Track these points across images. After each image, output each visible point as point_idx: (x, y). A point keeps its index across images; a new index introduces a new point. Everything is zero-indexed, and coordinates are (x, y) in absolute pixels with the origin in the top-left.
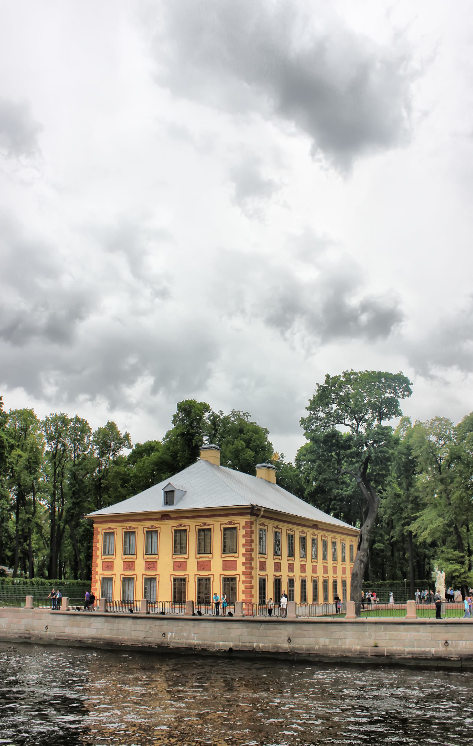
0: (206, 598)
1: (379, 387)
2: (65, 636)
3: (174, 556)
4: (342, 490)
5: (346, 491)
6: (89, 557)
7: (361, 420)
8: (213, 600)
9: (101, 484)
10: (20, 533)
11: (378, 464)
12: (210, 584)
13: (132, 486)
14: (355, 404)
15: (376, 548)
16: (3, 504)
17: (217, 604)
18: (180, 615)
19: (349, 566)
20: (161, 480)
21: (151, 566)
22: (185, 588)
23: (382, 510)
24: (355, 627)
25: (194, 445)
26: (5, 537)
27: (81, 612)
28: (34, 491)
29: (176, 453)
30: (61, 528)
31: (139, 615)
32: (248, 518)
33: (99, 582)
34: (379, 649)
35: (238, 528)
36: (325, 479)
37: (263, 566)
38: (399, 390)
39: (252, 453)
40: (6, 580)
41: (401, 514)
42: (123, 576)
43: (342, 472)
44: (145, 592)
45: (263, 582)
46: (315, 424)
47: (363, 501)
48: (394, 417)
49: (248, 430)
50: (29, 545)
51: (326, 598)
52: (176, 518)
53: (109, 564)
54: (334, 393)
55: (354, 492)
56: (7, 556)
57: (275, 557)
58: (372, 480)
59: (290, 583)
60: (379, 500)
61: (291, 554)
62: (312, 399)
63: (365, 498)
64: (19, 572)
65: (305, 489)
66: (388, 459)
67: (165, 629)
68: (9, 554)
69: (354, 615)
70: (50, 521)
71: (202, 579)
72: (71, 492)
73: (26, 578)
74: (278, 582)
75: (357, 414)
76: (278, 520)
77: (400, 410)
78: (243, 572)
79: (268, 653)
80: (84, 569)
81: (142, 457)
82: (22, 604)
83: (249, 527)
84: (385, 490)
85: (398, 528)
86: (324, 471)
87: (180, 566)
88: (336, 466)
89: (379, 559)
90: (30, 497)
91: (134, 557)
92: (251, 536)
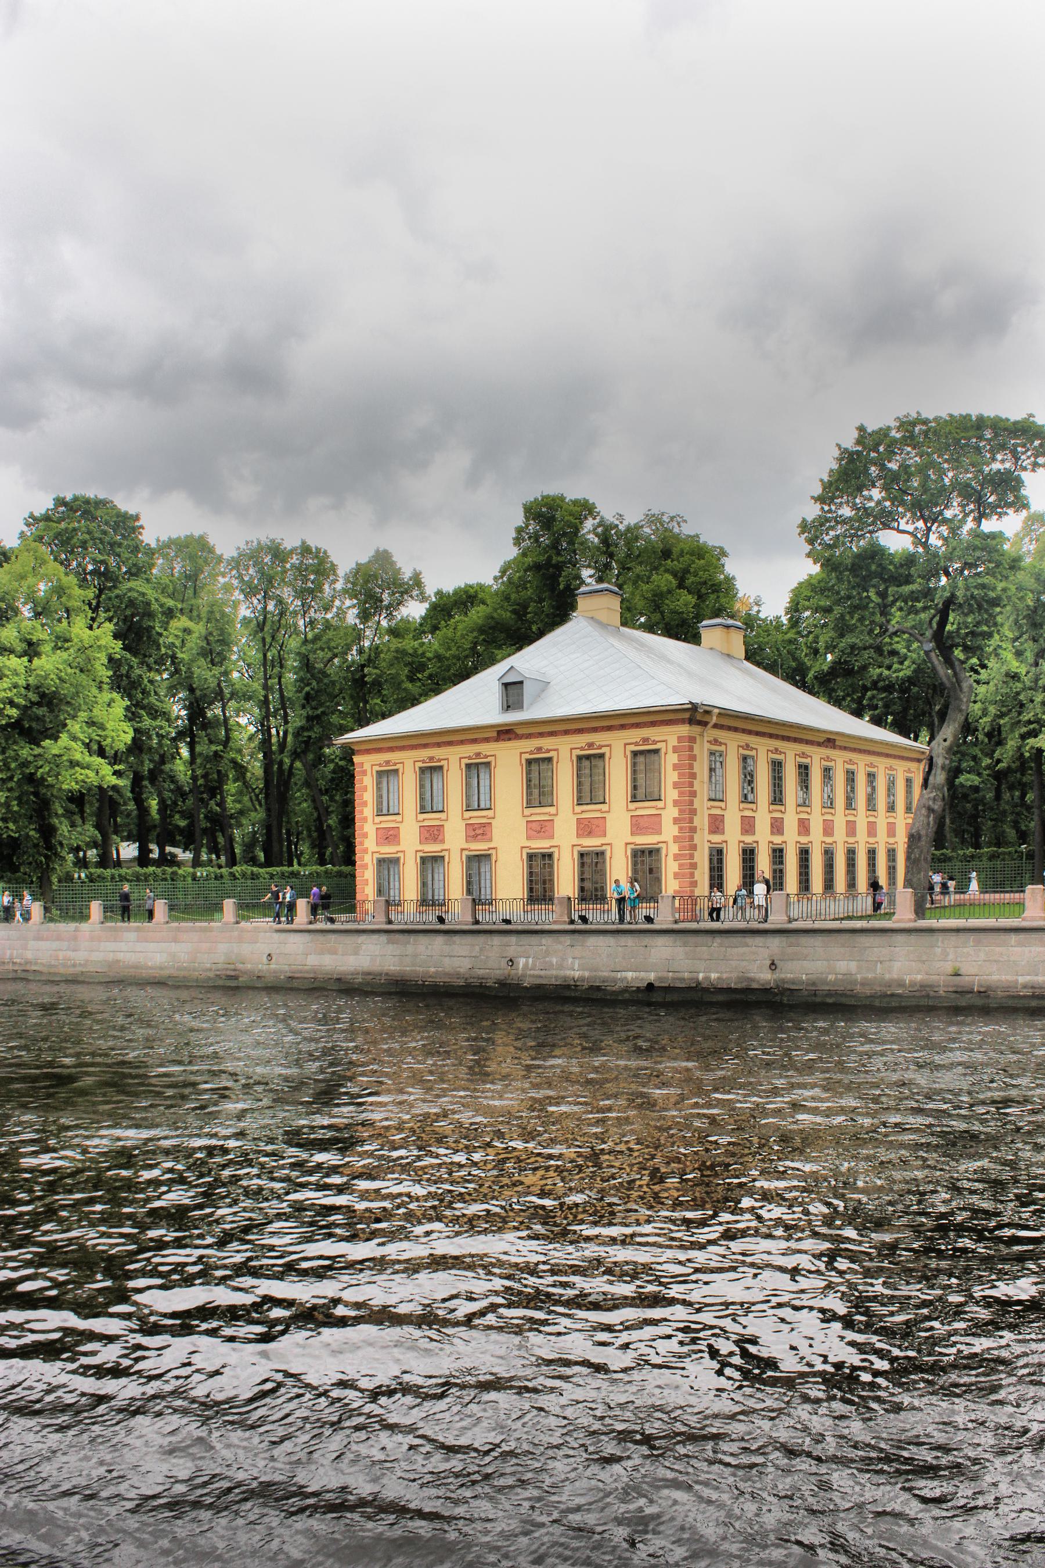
0: (596, 889)
1: (978, 449)
2: (307, 972)
3: (527, 812)
4: (889, 668)
5: (900, 670)
6: (348, 820)
7: (934, 521)
8: (611, 892)
9: (365, 676)
10: (201, 782)
11: (971, 612)
12: (604, 862)
13: (430, 677)
14: (924, 485)
15: (962, 785)
16: (161, 728)
17: (621, 901)
18: (544, 923)
19: (902, 822)
20: (493, 661)
21: (478, 831)
22: (551, 874)
23: (978, 705)
24: (913, 938)
25: (561, 587)
26: (171, 791)
27: (337, 926)
28: (222, 700)
29: (525, 607)
30: (286, 767)
31: (458, 927)
32: (684, 730)
34: (964, 981)
35: (663, 751)
36: (853, 647)
37: (717, 825)
38: (1023, 453)
39: (692, 599)
40: (180, 872)
41: (1020, 713)
42: (420, 854)
43: (891, 630)
44: (469, 883)
45: (717, 857)
46: (832, 533)
47: (938, 689)
48: (1010, 511)
49: (682, 551)
50: (221, 804)
51: (852, 884)
52: (529, 736)
54: (875, 464)
55: (915, 671)
56: (178, 826)
57: (742, 805)
58: (957, 646)
59: (774, 857)
60: (971, 687)
61: (777, 798)
62: (826, 478)
63: (942, 684)
64: (204, 857)
65: (809, 669)
66: (995, 602)
67: (511, 952)
68: (183, 823)
69: (913, 916)
70: (261, 756)
71: (588, 854)
72: (302, 695)
73: (220, 867)
74: (749, 856)
75: (927, 508)
76: (750, 732)
77: (1026, 497)
79: (729, 990)
80: (337, 843)
81: (451, 616)
82: (216, 916)
83: (687, 749)
84: (984, 666)
85: (1012, 744)
86: (851, 629)
87: (542, 829)
88: (878, 618)
89: (969, 806)
90: (215, 711)
91: (443, 816)
92: (691, 767)
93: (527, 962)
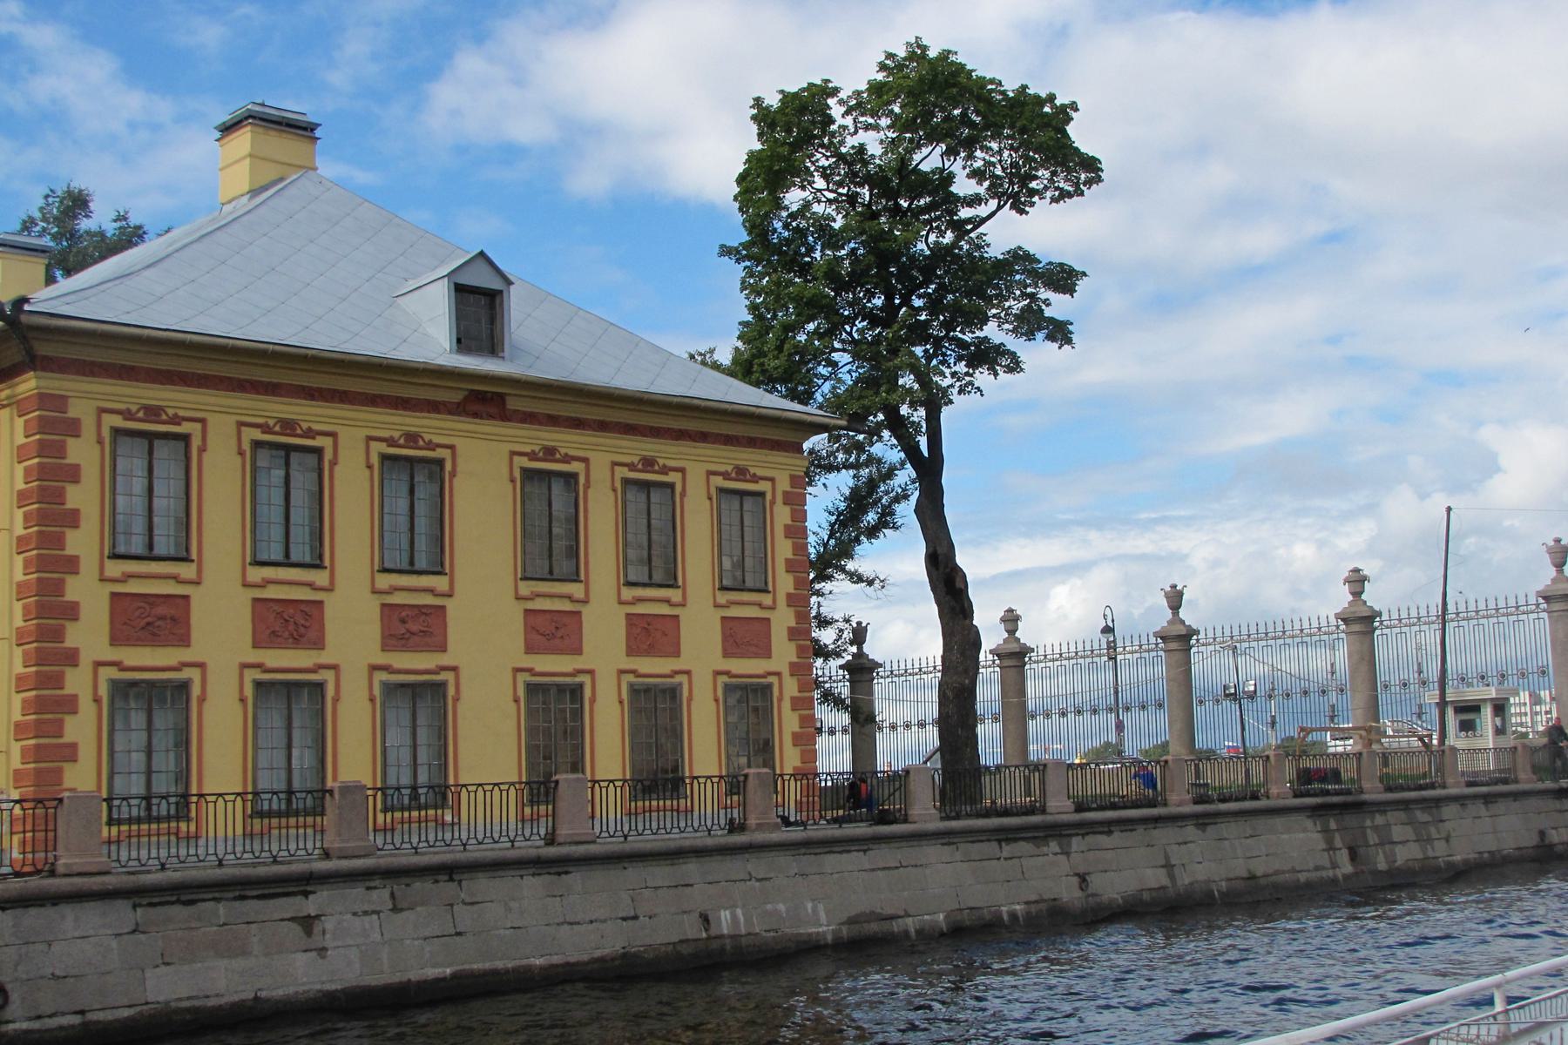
3: (525, 588)
21: (414, 626)
33: (86, 706)
42: (251, 675)
53: (161, 610)
78: (792, 665)
87: (553, 631)
93: (734, 917)
